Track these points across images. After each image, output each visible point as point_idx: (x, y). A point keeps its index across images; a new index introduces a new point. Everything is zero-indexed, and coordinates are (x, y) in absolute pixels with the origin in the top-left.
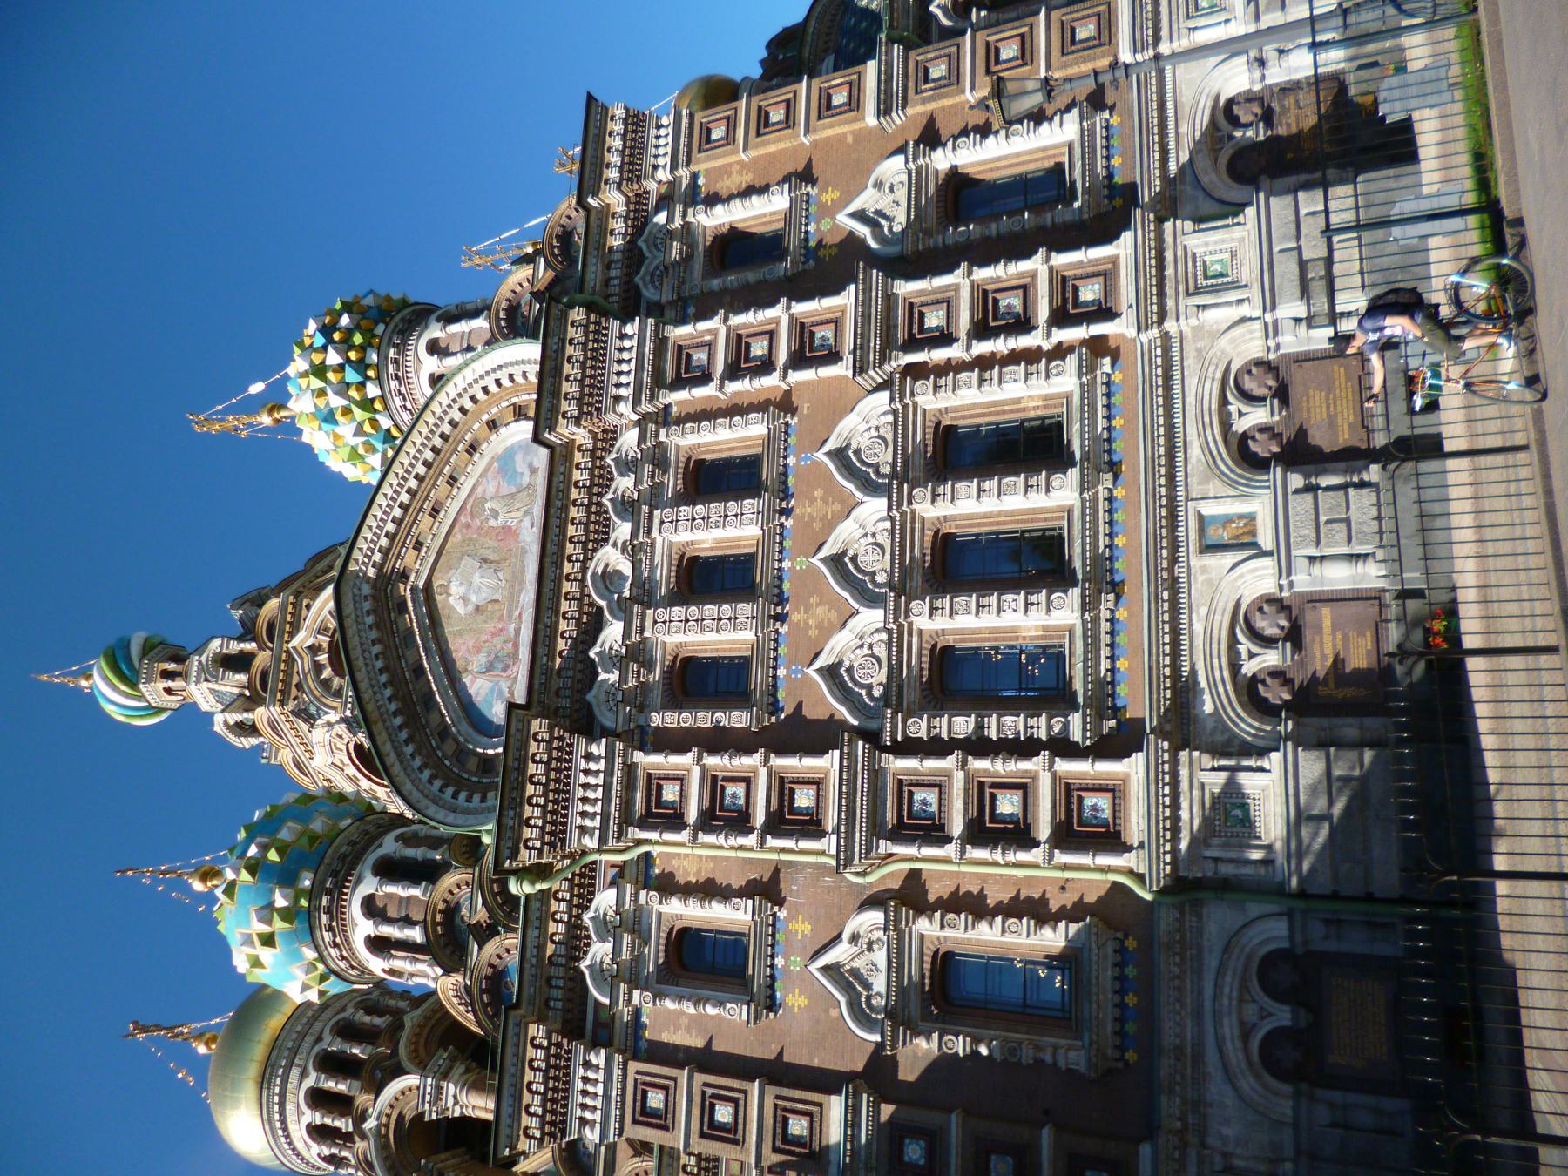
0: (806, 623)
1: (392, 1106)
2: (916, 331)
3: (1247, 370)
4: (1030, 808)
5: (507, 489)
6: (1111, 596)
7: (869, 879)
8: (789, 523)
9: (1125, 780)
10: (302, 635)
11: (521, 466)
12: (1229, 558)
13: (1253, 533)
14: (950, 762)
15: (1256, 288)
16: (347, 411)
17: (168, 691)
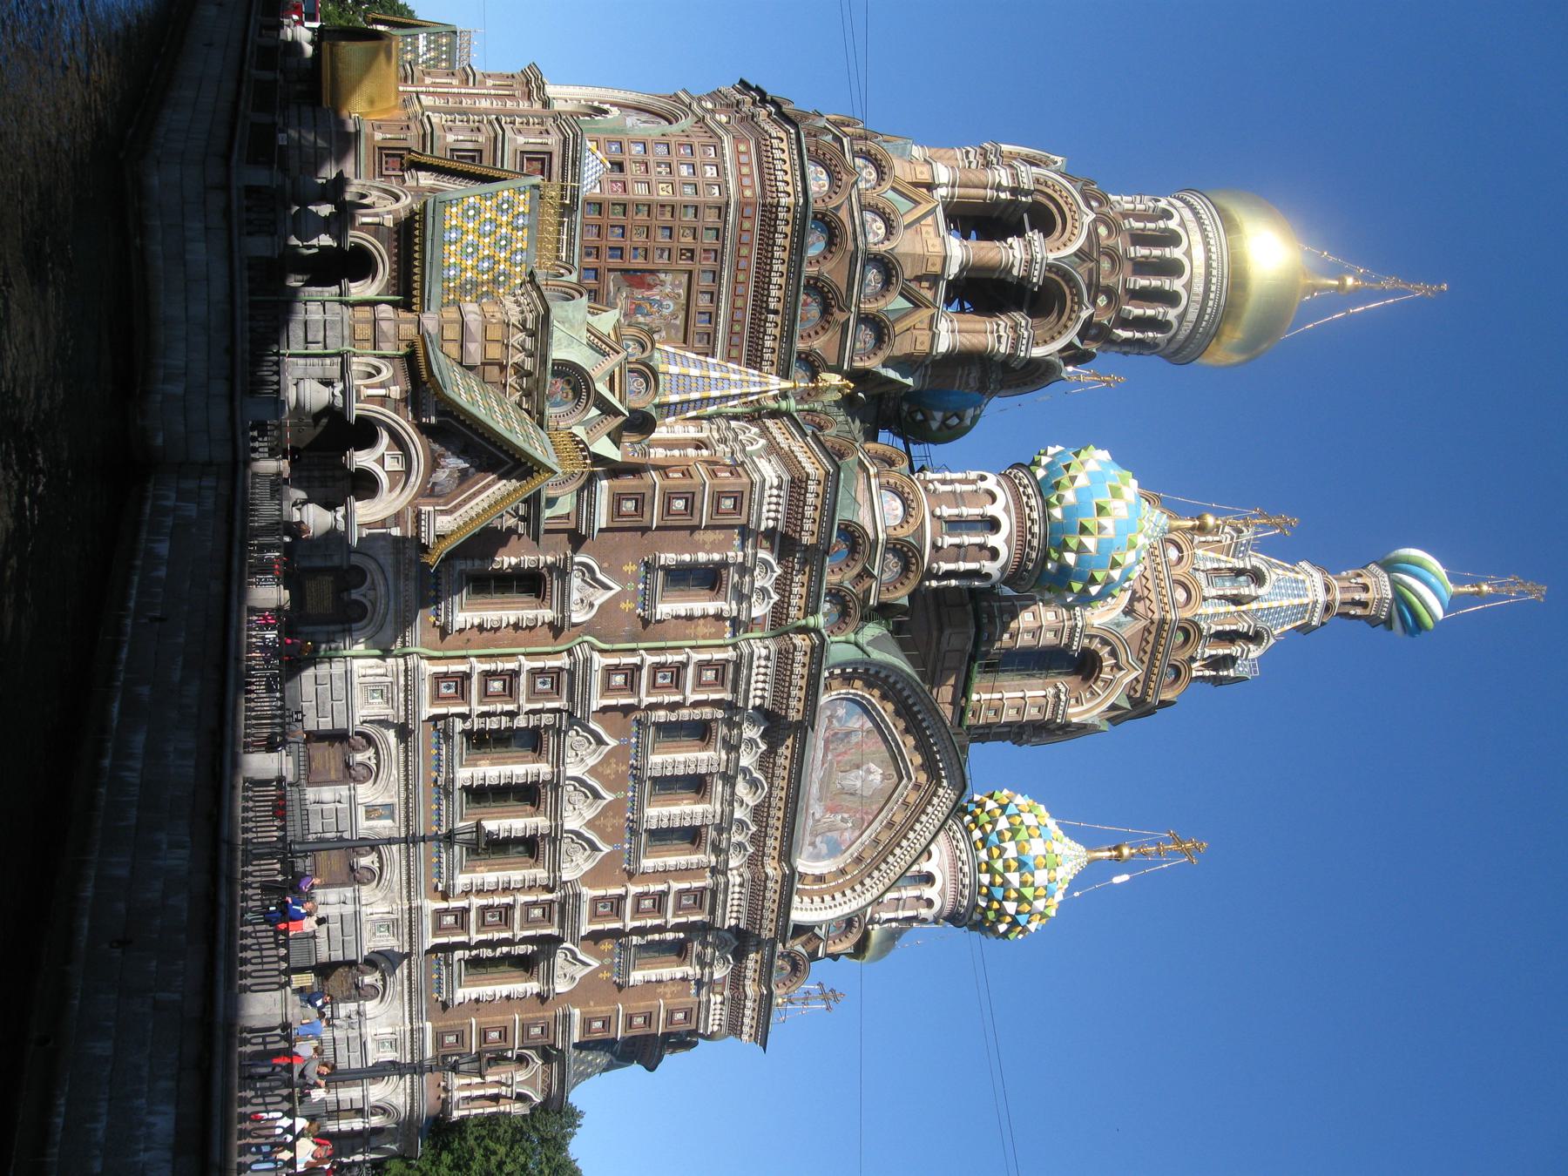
0: (617, 765)
1: (1066, 327)
2: (547, 910)
3: (369, 882)
4: (483, 687)
5: (835, 834)
6: (439, 783)
7: (580, 640)
8: (629, 814)
9: (432, 704)
10: (1127, 680)
11: (823, 848)
12: (379, 802)
13: (366, 811)
14: (528, 707)
15: (363, 920)
16: (1007, 868)
17: (1365, 588)
